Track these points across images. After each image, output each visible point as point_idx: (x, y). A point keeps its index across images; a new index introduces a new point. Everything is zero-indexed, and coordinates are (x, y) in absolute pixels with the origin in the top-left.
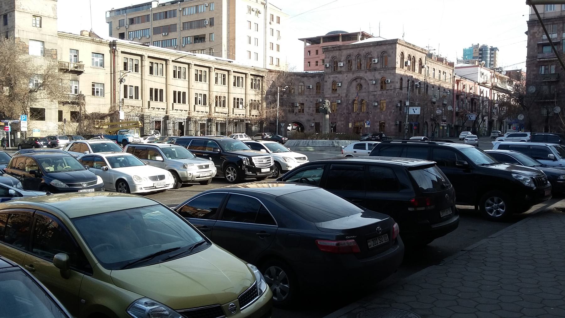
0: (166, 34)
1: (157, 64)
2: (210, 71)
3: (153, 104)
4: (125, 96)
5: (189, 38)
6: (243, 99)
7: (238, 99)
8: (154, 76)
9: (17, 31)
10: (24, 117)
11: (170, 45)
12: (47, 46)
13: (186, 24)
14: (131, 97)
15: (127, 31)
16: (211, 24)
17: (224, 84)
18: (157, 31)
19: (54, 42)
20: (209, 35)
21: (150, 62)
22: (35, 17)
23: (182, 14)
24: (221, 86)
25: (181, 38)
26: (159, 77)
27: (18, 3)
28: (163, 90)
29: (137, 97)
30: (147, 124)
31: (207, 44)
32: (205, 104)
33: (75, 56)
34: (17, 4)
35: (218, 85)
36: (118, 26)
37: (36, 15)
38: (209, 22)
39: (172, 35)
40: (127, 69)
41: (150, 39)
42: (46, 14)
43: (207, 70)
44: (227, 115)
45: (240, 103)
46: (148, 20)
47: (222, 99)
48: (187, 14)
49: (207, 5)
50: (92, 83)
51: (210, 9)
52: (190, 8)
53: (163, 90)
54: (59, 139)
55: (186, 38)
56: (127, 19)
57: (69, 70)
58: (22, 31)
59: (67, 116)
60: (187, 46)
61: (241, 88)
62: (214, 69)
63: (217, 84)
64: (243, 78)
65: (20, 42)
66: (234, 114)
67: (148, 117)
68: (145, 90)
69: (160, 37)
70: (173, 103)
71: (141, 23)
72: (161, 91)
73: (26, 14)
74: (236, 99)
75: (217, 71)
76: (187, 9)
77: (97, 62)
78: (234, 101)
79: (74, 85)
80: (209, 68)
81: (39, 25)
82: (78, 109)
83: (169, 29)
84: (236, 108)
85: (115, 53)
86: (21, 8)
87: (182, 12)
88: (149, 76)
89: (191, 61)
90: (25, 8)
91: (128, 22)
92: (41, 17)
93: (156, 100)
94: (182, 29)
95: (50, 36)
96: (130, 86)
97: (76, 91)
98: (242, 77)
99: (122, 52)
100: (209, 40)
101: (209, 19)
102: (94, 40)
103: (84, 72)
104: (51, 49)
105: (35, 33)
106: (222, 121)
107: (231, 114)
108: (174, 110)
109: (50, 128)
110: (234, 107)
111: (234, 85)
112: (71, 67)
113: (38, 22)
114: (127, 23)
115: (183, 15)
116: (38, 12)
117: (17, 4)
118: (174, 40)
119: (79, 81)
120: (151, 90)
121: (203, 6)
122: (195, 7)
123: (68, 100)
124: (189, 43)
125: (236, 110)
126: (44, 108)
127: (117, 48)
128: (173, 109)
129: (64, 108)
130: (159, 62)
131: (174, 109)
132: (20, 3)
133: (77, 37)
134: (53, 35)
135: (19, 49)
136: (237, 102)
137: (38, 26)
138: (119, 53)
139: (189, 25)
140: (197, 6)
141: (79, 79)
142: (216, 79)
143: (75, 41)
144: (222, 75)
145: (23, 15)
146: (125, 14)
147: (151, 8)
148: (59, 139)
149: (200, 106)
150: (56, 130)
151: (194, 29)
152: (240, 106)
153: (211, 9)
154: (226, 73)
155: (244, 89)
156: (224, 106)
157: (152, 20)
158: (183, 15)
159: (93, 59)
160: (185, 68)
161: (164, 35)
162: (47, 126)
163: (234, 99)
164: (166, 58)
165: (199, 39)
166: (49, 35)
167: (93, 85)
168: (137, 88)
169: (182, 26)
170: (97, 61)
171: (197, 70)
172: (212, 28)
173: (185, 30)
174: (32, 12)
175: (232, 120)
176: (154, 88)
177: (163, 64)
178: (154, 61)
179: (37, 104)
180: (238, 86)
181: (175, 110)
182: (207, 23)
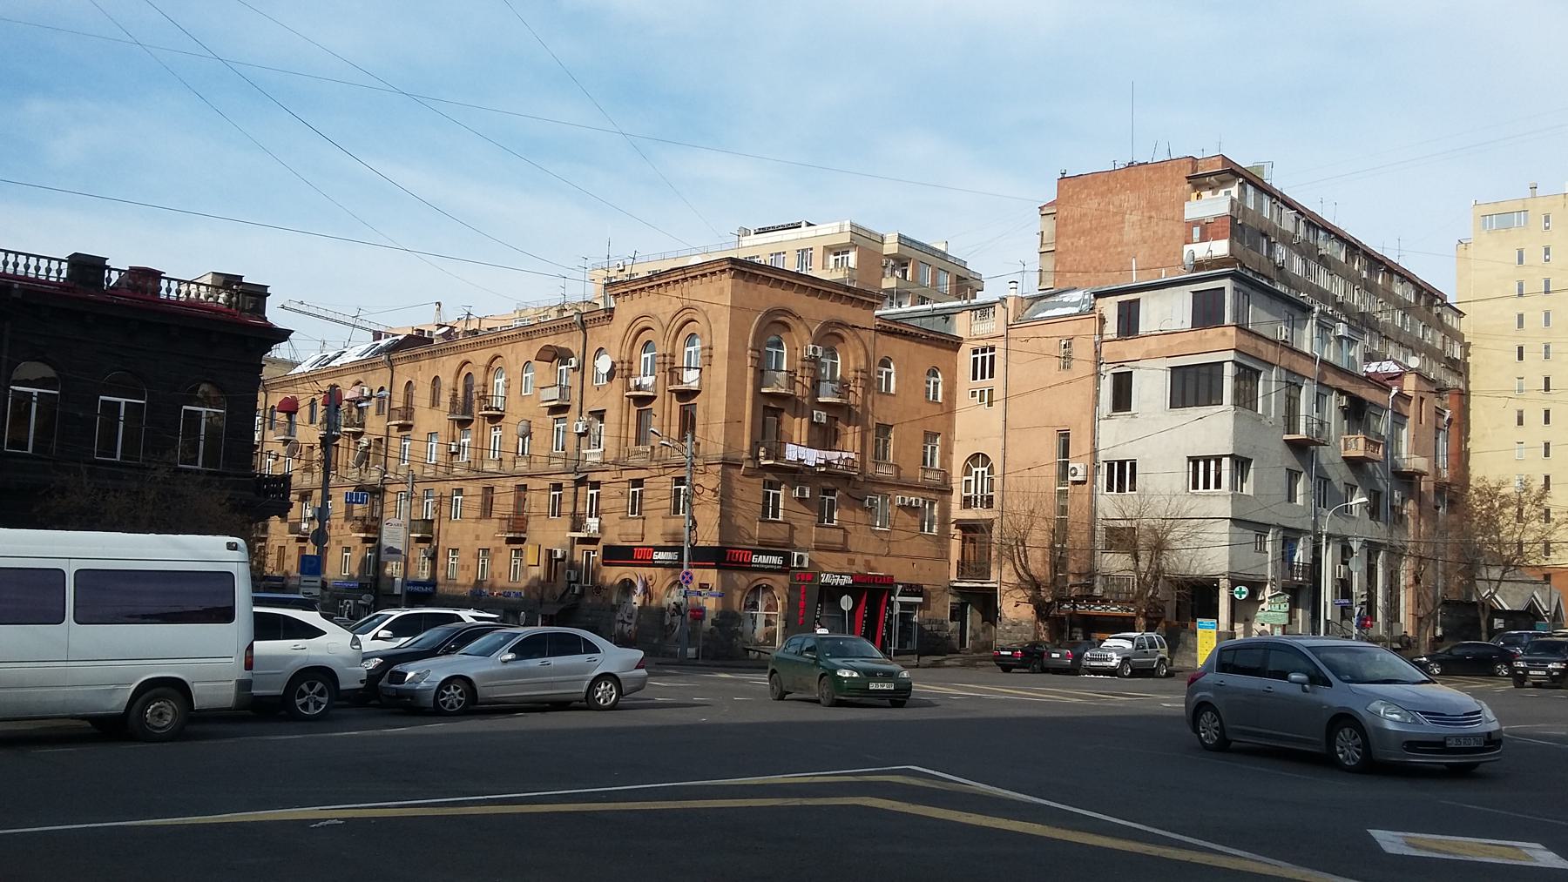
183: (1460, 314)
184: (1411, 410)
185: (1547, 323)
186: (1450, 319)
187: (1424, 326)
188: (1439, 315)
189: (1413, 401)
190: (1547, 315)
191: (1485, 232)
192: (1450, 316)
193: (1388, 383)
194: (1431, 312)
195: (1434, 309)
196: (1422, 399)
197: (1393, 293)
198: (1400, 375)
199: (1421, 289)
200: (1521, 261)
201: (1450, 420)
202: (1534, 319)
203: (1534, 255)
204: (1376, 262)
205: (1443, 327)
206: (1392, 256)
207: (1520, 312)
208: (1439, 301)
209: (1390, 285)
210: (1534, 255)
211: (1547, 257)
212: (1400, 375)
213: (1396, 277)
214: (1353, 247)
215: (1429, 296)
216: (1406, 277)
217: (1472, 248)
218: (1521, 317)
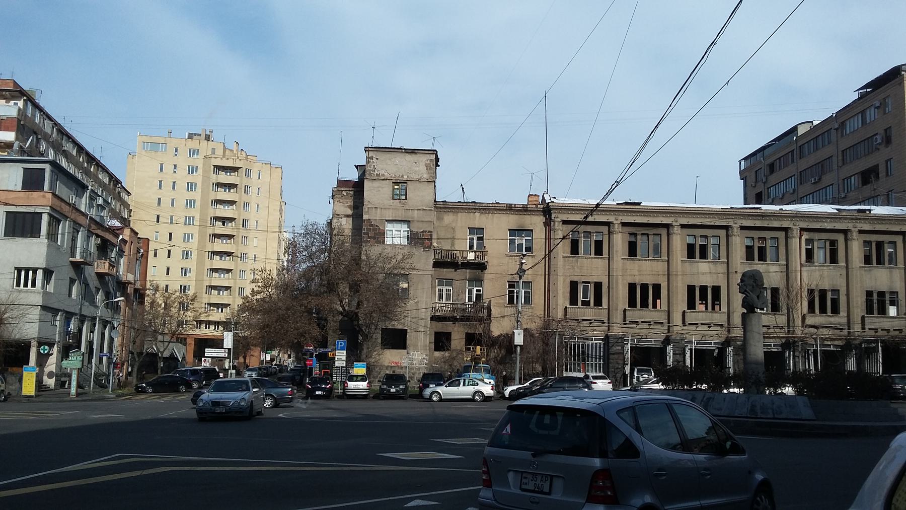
0: (817, 180)
1: (648, 235)
2: (787, 238)
3: (635, 314)
4: (573, 300)
5: (853, 178)
6: (897, 292)
7: (881, 294)
8: (639, 260)
9: (366, 209)
10: (341, 344)
11: (818, 200)
12: (417, 228)
13: (848, 150)
14: (586, 304)
15: (766, 188)
16: (888, 140)
17: (834, 259)
18: (802, 177)
19: (427, 220)
20: (884, 165)
21: (631, 234)
22: (398, 184)
23: (839, 135)
24: (824, 266)
25: (841, 181)
26: (651, 260)
27: (370, 167)
28: (660, 284)
29: (598, 302)
30: (616, 356)
31: (882, 184)
32: (775, 308)
33: (479, 239)
34: (369, 168)
35: (816, 266)
36: (754, 180)
37: (398, 181)
38: (884, 137)
39: (827, 179)
40: (882, 261)
41: (796, 193)
42: (415, 177)
43: (781, 235)
44: (845, 332)
45: (888, 302)
46: (793, 161)
47: (829, 296)
48: (848, 132)
49: (878, 105)
50: (508, 281)
51: (885, 110)
52: (852, 120)
53: (660, 284)
54: (347, 381)
55: (849, 180)
56: (765, 166)
57: (460, 263)
58: (374, 209)
59: (458, 340)
60: (851, 194)
61: (888, 268)
62: (796, 233)
63: (809, 264)
64: (895, 242)
65: (372, 225)
66: (867, 329)
67: (620, 340)
68: (613, 288)
69: (807, 188)
70: (686, 309)
71: (784, 167)
72: (657, 288)
73: (381, 181)
74: (875, 296)
75: (805, 236)
76: (848, 123)
77: (520, 245)
78: (866, 299)
79: (475, 289)
80: (786, 230)
81: (404, 196)
82: (480, 330)
83: (822, 167)
84: (876, 315)
85: (550, 226)
86: (374, 174)
87: (840, 131)
88: (627, 259)
89: (730, 220)
90: (382, 172)
91: (767, 171)
92: (407, 183)
93: (644, 305)
94: (840, 164)
95: (421, 211)
96: (583, 282)
97: (479, 297)
98: (890, 242)
99: (565, 222)
100: (884, 174)
101: (883, 132)
102: (513, 208)
103: (486, 264)
104: (422, 230)
105: (394, 209)
106: (830, 345)
107: (857, 328)
108: (687, 324)
109: (414, 362)
110: (870, 310)
111: (867, 260)
112: (471, 256)
113: (403, 192)
114: (765, 172)
115: (842, 136)
116: (403, 176)
117: (369, 168)
118: (831, 187)
119: (483, 280)
120: (632, 287)
121: (872, 109)
122: (860, 116)
123: (455, 315)
124: (853, 189)
125: (875, 322)
126: (406, 328)
127: (553, 216)
128: (684, 322)
129: (456, 329)
130: (651, 231)
131: (687, 321)
132: (374, 166)
133: (481, 207)
134: (425, 208)
135: (369, 237)
136: (878, 300)
137: (403, 197)
138: (556, 223)
139: (846, 156)
140: (863, 112)
141: (483, 277)
142: (810, 254)
143: (477, 214)
144: (828, 244)
145: (376, 184)
146: (762, 158)
147: (795, 138)
148: (347, 381)
149: (764, 314)
150: (424, 365)
151: (861, 157)
152: (892, 311)
153: (887, 112)
154: (840, 238)
155: (899, 268)
156: (835, 310)
157: (798, 159)
158: (842, 136)
159: (512, 241)
160: (719, 236)
161: (813, 182)
162: (410, 358)
163: (869, 294)
164: (666, 221)
165: (868, 176)
166: (420, 208)
167: (510, 286)
168: (598, 286)
169: (840, 158)
170: (520, 242)
171: (753, 238)
172: (890, 148)
173: (847, 163)
174: (392, 177)
175: (857, 342)
176: (638, 280)
177: (661, 234)
178: (639, 231)
179: (396, 323)
180: (880, 262)
181: (689, 324)
182: (879, 141)
183: (129, 193)
184: (126, 248)
185: (173, 205)
186: (123, 195)
187: (111, 198)
188: (119, 193)
189: (128, 244)
190: (173, 200)
191: (144, 151)
192: (124, 194)
193: (117, 232)
194: (115, 190)
195: (117, 189)
196: (132, 242)
197: (98, 178)
198: (122, 228)
199: (111, 177)
200: (161, 170)
201: (142, 255)
202: (166, 202)
203: (169, 168)
204: (91, 159)
205: (120, 200)
206: (97, 157)
207: (159, 197)
208: (120, 185)
209: (97, 172)
210: (169, 168)
211: (175, 170)
212: (122, 228)
213: (100, 169)
214: (81, 149)
215: (115, 181)
216: (105, 170)
217: (136, 158)
218: (159, 199)
